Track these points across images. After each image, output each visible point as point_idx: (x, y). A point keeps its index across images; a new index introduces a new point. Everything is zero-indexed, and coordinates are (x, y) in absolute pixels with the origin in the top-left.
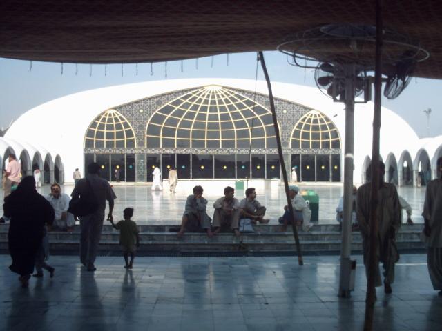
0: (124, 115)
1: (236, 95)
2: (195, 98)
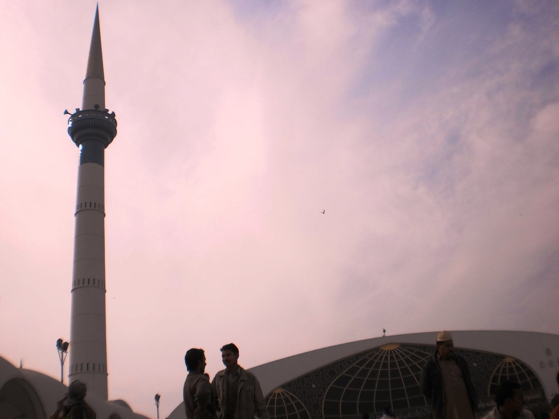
1: (417, 353)
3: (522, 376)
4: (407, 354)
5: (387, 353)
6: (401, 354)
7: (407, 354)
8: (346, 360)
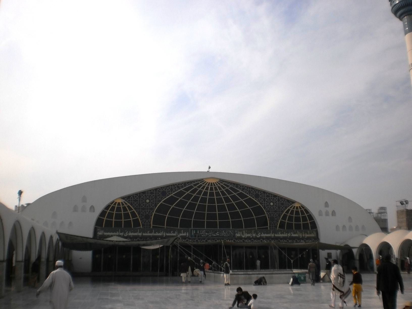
0: (131, 204)
1: (231, 188)
2: (196, 190)
3: (304, 219)
4: (224, 188)
5: (209, 185)
6: (219, 187)
7: (224, 188)
8: (176, 184)
